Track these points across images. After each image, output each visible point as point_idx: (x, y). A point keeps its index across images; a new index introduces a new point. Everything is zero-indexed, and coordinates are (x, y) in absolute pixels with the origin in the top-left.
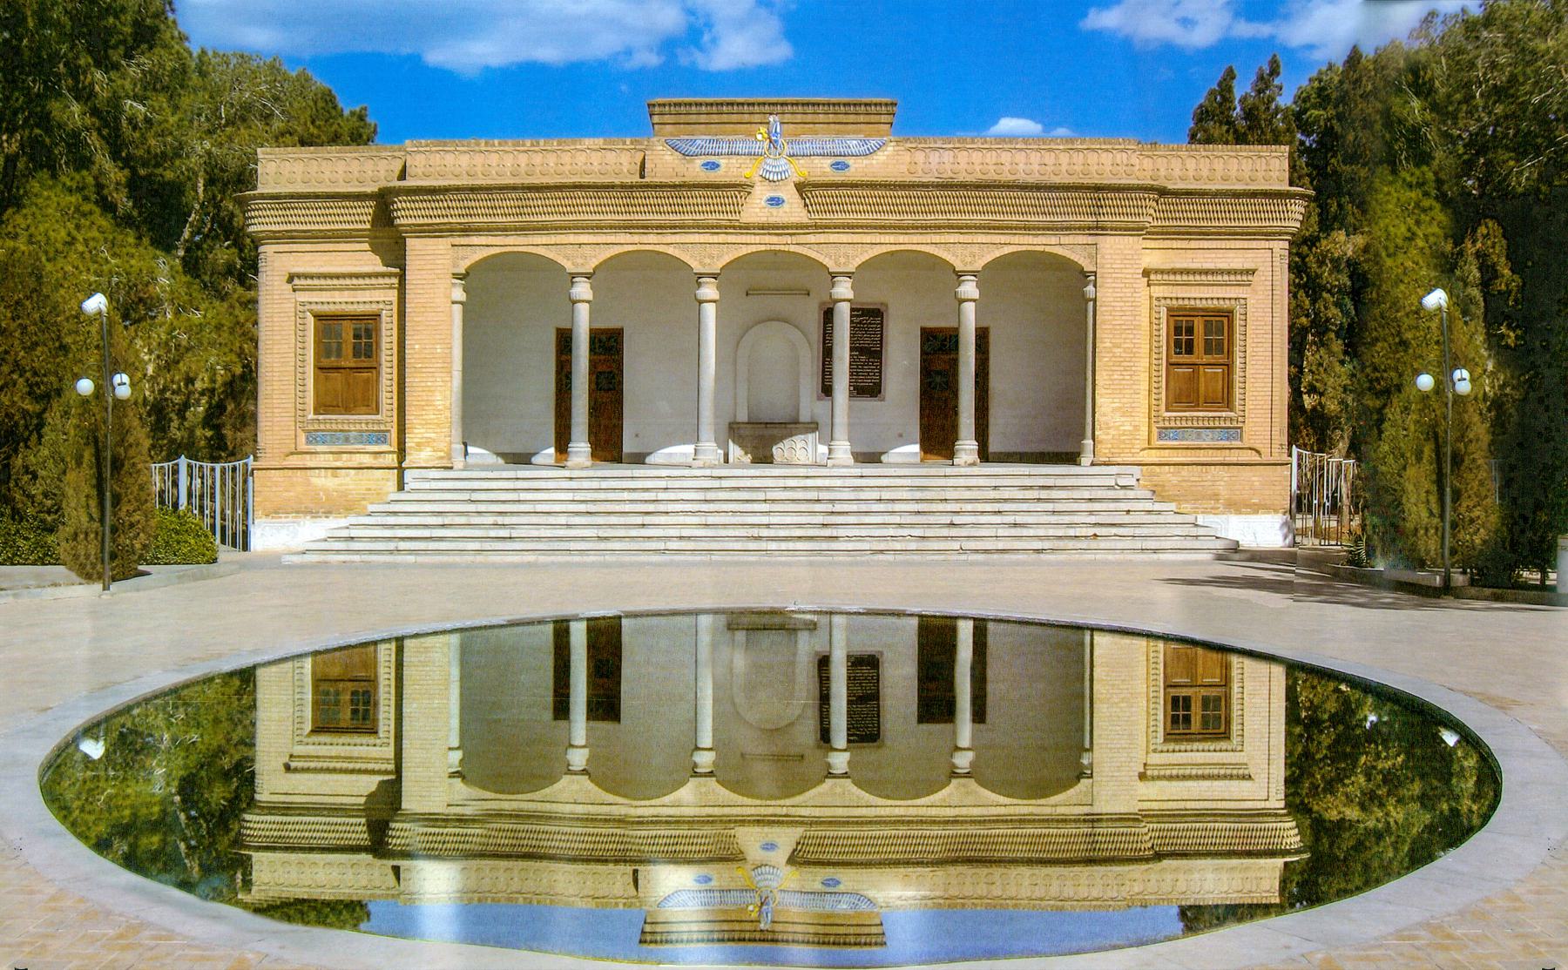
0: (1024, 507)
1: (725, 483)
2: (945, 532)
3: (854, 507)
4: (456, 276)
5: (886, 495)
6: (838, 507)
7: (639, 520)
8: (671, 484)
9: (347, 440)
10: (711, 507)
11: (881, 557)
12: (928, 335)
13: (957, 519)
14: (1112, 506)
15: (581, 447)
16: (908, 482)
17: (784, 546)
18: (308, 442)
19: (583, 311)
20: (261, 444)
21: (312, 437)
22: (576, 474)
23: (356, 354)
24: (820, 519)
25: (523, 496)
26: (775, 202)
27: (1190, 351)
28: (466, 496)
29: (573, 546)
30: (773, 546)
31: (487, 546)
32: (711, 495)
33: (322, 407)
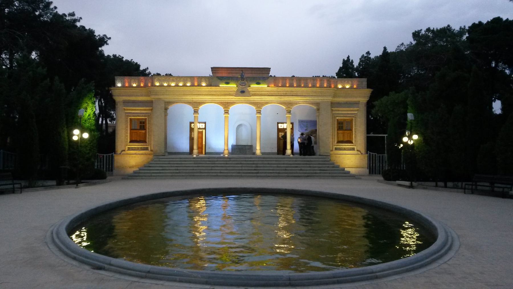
0: (303, 165)
2: (284, 171)
3: (262, 165)
5: (270, 162)
6: (259, 165)
7: (210, 168)
13: (287, 169)
17: (245, 175)
20: (116, 150)
24: (253, 168)
30: (243, 175)
31: (173, 174)
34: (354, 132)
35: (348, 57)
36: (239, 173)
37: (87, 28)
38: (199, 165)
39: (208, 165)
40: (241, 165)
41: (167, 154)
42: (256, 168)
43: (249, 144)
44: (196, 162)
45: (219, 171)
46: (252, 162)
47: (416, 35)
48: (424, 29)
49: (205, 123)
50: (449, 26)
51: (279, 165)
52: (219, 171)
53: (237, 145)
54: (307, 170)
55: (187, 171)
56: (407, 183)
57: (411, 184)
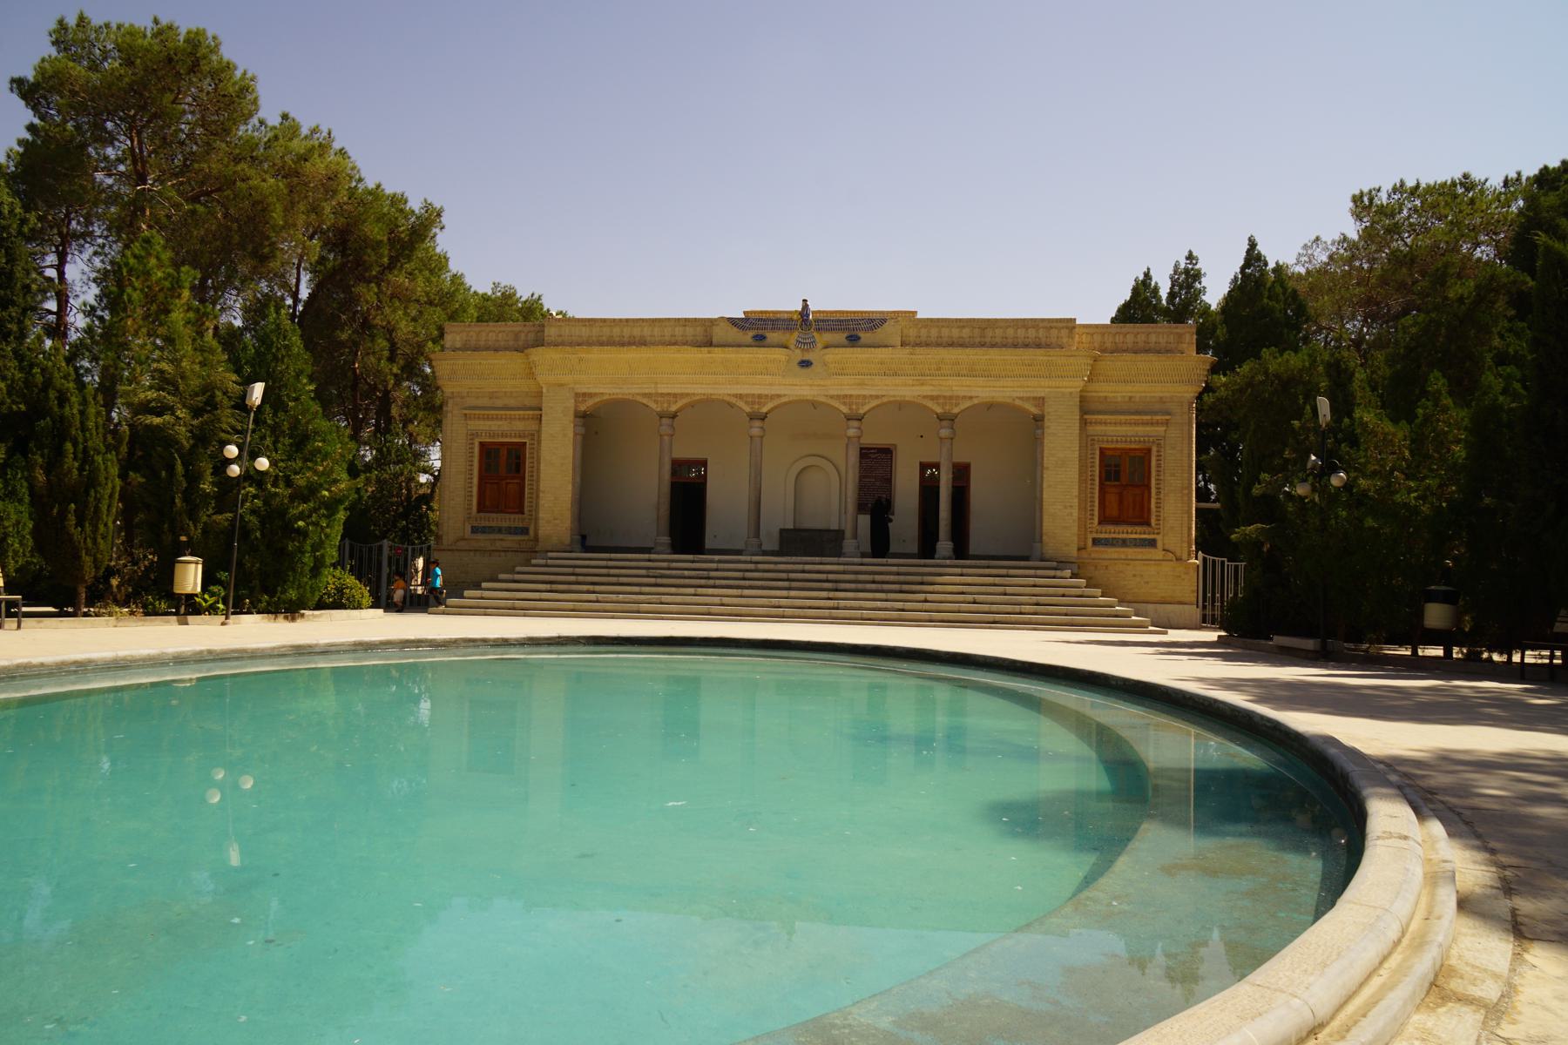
0: (983, 589)
1: (761, 566)
5: (877, 578)
9: (500, 530)
10: (747, 583)
12: (924, 467)
14: (1051, 590)
16: (894, 569)
21: (474, 530)
26: (805, 364)
27: (1117, 478)
28: (570, 570)
32: (748, 575)
33: (482, 508)
34: (1153, 491)
35: (1147, 275)
38: (659, 581)
43: (834, 526)
44: (652, 572)
45: (717, 600)
46: (823, 576)
47: (1362, 204)
48: (1387, 186)
50: (1466, 176)
52: (717, 600)
53: (795, 530)
56: (1310, 644)
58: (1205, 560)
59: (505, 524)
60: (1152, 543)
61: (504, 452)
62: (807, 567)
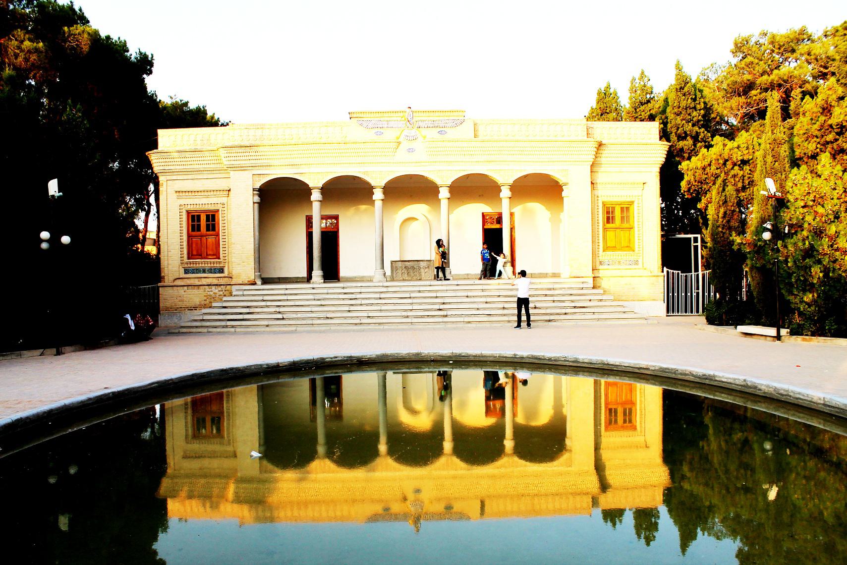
1: (390, 289)
2: (501, 312)
4: (254, 190)
8: (363, 290)
9: (204, 271)
11: (469, 325)
15: (317, 273)
18: (186, 273)
19: (316, 206)
21: (187, 271)
22: (314, 286)
23: (208, 230)
24: (437, 307)
25: (290, 297)
26: (410, 150)
29: (315, 322)
31: (271, 323)
32: (382, 296)
36: (408, 317)
37: (103, 35)
38: (323, 303)
39: (342, 302)
40: (410, 301)
41: (259, 282)
42: (442, 307)
44: (317, 297)
46: (434, 295)
47: (740, 47)
49: (336, 218)
51: (489, 300)
54: (547, 308)
55: (299, 315)
56: (772, 331)
57: (778, 332)
58: (668, 272)
59: (208, 266)
60: (636, 263)
61: (203, 218)
62: (422, 289)
